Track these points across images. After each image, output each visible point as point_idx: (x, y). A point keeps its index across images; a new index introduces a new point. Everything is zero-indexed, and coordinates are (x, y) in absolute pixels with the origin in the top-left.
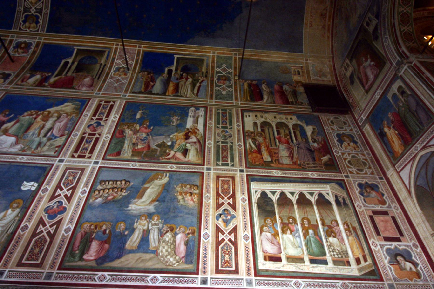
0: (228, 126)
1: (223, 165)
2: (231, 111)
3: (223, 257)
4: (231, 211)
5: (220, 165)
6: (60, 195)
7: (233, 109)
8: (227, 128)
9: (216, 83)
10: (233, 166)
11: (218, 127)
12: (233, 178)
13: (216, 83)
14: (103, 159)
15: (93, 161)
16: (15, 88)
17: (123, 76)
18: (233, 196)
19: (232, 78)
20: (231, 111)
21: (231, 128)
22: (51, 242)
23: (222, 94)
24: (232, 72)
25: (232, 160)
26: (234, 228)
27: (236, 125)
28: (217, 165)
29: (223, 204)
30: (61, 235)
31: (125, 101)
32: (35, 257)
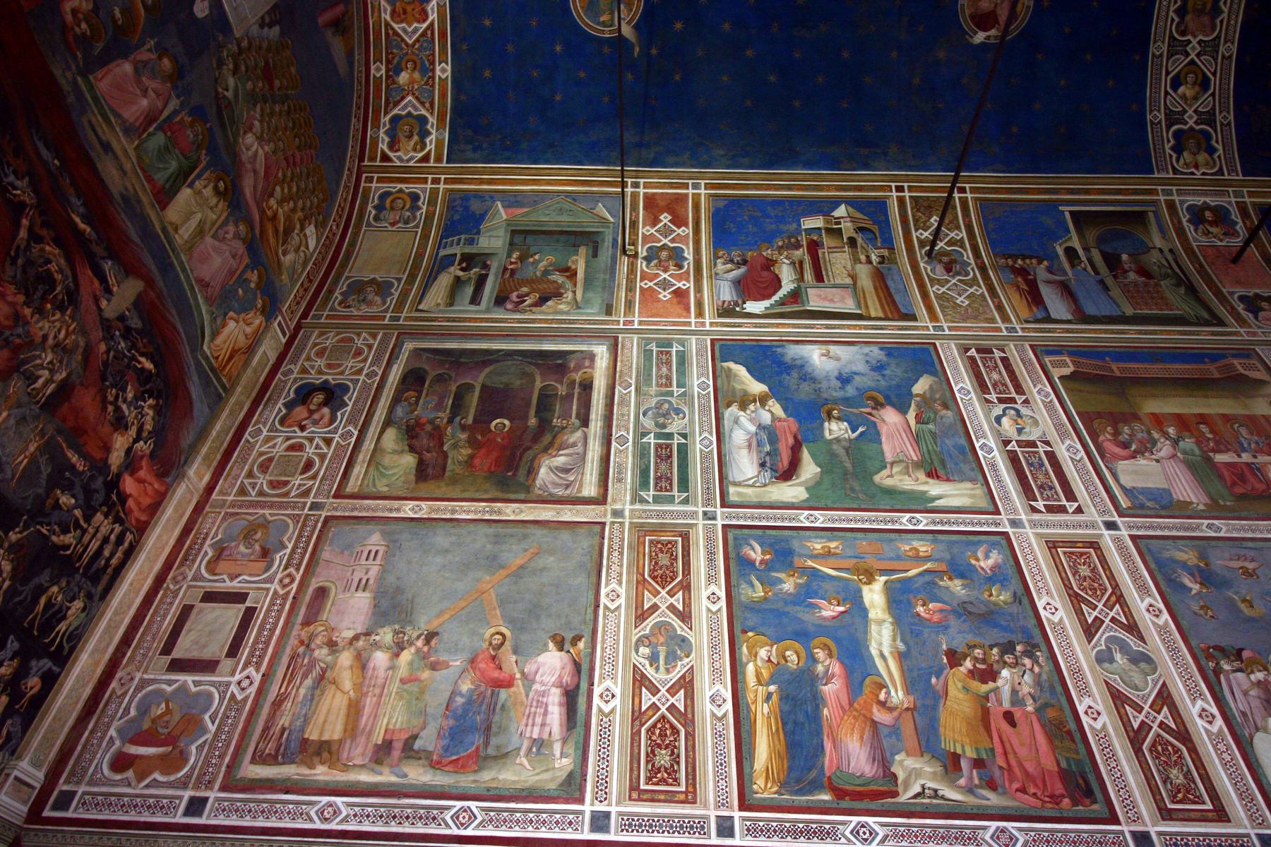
0: (1014, 395)
1: (1050, 509)
2: (1004, 351)
3: (1187, 776)
4: (1131, 643)
5: (1041, 512)
6: (655, 608)
7: (1008, 345)
8: (1013, 400)
9: (927, 274)
10: (1079, 510)
12: (1095, 545)
14: (723, 506)
15: (701, 510)
16: (416, 319)
17: (673, 270)
18: (1120, 599)
19: (968, 258)
21: (1026, 402)
22: (690, 736)
23: (960, 306)
24: (962, 240)
25: (1071, 496)
26: (1159, 693)
27: (1035, 391)
28: (1034, 510)
29: (1098, 621)
30: (708, 714)
31: (708, 339)
32: (666, 775)
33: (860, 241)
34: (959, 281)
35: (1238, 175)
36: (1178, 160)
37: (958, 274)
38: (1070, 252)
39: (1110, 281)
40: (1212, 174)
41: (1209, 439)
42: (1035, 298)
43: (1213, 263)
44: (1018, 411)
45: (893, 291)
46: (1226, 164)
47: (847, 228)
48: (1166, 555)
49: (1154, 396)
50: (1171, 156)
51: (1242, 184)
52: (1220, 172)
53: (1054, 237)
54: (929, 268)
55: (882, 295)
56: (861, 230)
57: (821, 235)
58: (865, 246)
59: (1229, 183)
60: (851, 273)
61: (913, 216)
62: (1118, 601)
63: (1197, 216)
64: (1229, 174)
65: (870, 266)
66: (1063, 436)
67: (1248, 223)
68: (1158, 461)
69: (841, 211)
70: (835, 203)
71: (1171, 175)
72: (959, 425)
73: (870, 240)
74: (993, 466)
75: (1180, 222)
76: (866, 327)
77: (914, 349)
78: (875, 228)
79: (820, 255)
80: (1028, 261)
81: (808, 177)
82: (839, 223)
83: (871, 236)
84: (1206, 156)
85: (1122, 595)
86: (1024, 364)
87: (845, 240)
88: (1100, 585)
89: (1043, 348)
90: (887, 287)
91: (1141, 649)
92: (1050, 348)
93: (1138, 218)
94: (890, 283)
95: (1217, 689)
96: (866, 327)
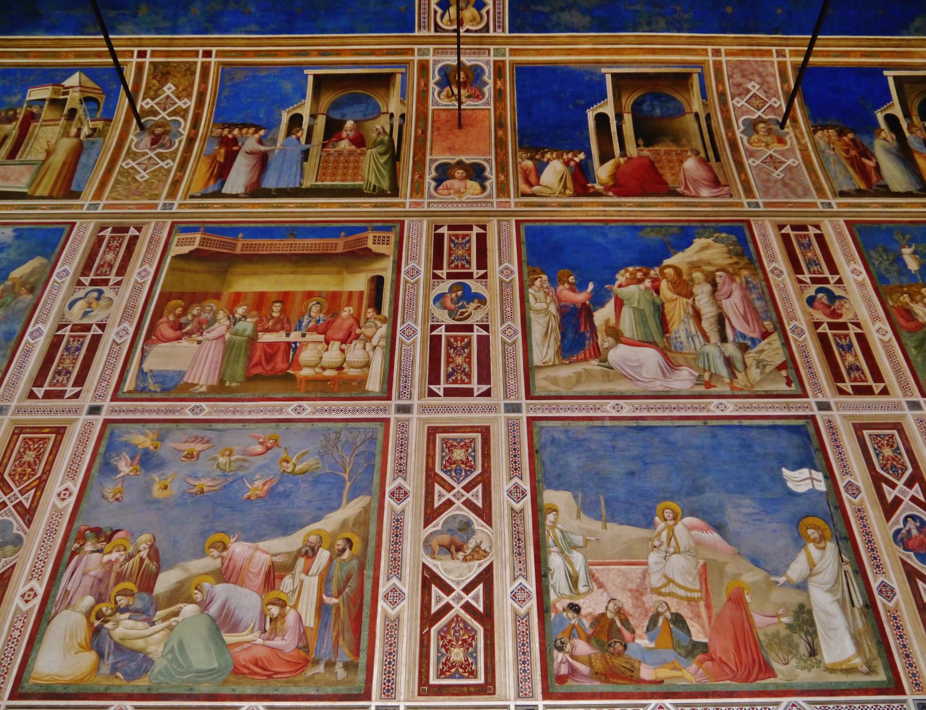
11: (80, 283)
13: (130, 147)
20: (139, 229)
28: (32, 395)
33: (80, 112)
34: (158, 155)
35: (503, 31)
36: (442, 16)
37: (163, 146)
38: (296, 120)
39: (315, 151)
40: (476, 31)
41: (273, 317)
42: (222, 171)
43: (438, 129)
44: (101, 292)
45: (79, 166)
46: (494, 20)
47: (73, 99)
48: (125, 438)
49: (255, 274)
50: (436, 12)
51: (506, 41)
52: (486, 29)
53: (285, 102)
54: (136, 140)
55: (65, 171)
56: (87, 100)
57: (42, 107)
58: (83, 117)
59: (493, 41)
60: (51, 148)
61: (147, 83)
62: (37, 487)
63: (448, 78)
64: (495, 31)
65: (75, 140)
66: (125, 317)
67: (499, 83)
68: (199, 342)
69: (74, 80)
70: (69, 71)
71: (432, 33)
72: (31, 307)
73: (91, 111)
74: (27, 353)
75: (427, 85)
76: (27, 207)
77: (48, 230)
78: (102, 99)
79: (31, 129)
80: (244, 131)
81: (48, 43)
82: (67, 93)
83: (95, 106)
84: (474, 11)
85: (46, 481)
86: (150, 242)
87: (66, 111)
88: (34, 470)
89: (184, 225)
90: (76, 162)
91: (21, 533)
92: (191, 225)
93: (383, 81)
94: (83, 159)
95: (61, 569)
96: (19, 207)
